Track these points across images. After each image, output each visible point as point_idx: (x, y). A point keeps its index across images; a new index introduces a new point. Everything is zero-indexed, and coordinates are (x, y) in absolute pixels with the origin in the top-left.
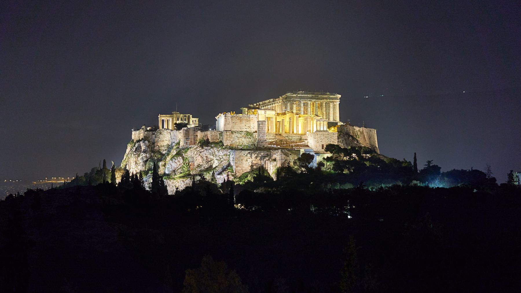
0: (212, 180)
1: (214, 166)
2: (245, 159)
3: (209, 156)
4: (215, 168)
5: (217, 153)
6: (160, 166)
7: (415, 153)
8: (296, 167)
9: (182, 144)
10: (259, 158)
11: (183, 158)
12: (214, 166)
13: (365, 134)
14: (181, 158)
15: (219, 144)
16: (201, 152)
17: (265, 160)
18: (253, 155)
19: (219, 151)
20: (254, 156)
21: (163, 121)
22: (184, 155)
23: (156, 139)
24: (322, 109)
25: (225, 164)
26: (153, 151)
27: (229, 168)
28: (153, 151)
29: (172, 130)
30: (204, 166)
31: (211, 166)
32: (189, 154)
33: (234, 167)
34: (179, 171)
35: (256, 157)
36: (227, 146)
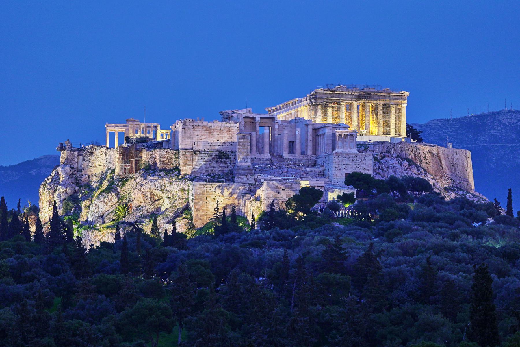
0: (153, 232)
1: (163, 209)
2: (212, 197)
3: (155, 192)
4: (164, 212)
5: (168, 186)
6: (83, 209)
7: (510, 190)
8: (290, 211)
9: (117, 171)
10: (235, 196)
11: (118, 194)
12: (163, 209)
13: (442, 157)
14: (113, 194)
15: (172, 171)
16: (142, 185)
17: (245, 198)
18: (226, 190)
19: (171, 183)
20: (227, 192)
21: (112, 134)
22: (119, 190)
23: (85, 163)
24: (377, 116)
25: (180, 205)
26: (78, 183)
27: (186, 211)
28: (78, 184)
29: (108, 149)
30: (148, 208)
31: (159, 209)
32: (129, 187)
33: (193, 211)
34: (110, 216)
35: (231, 194)
36: (186, 174)
